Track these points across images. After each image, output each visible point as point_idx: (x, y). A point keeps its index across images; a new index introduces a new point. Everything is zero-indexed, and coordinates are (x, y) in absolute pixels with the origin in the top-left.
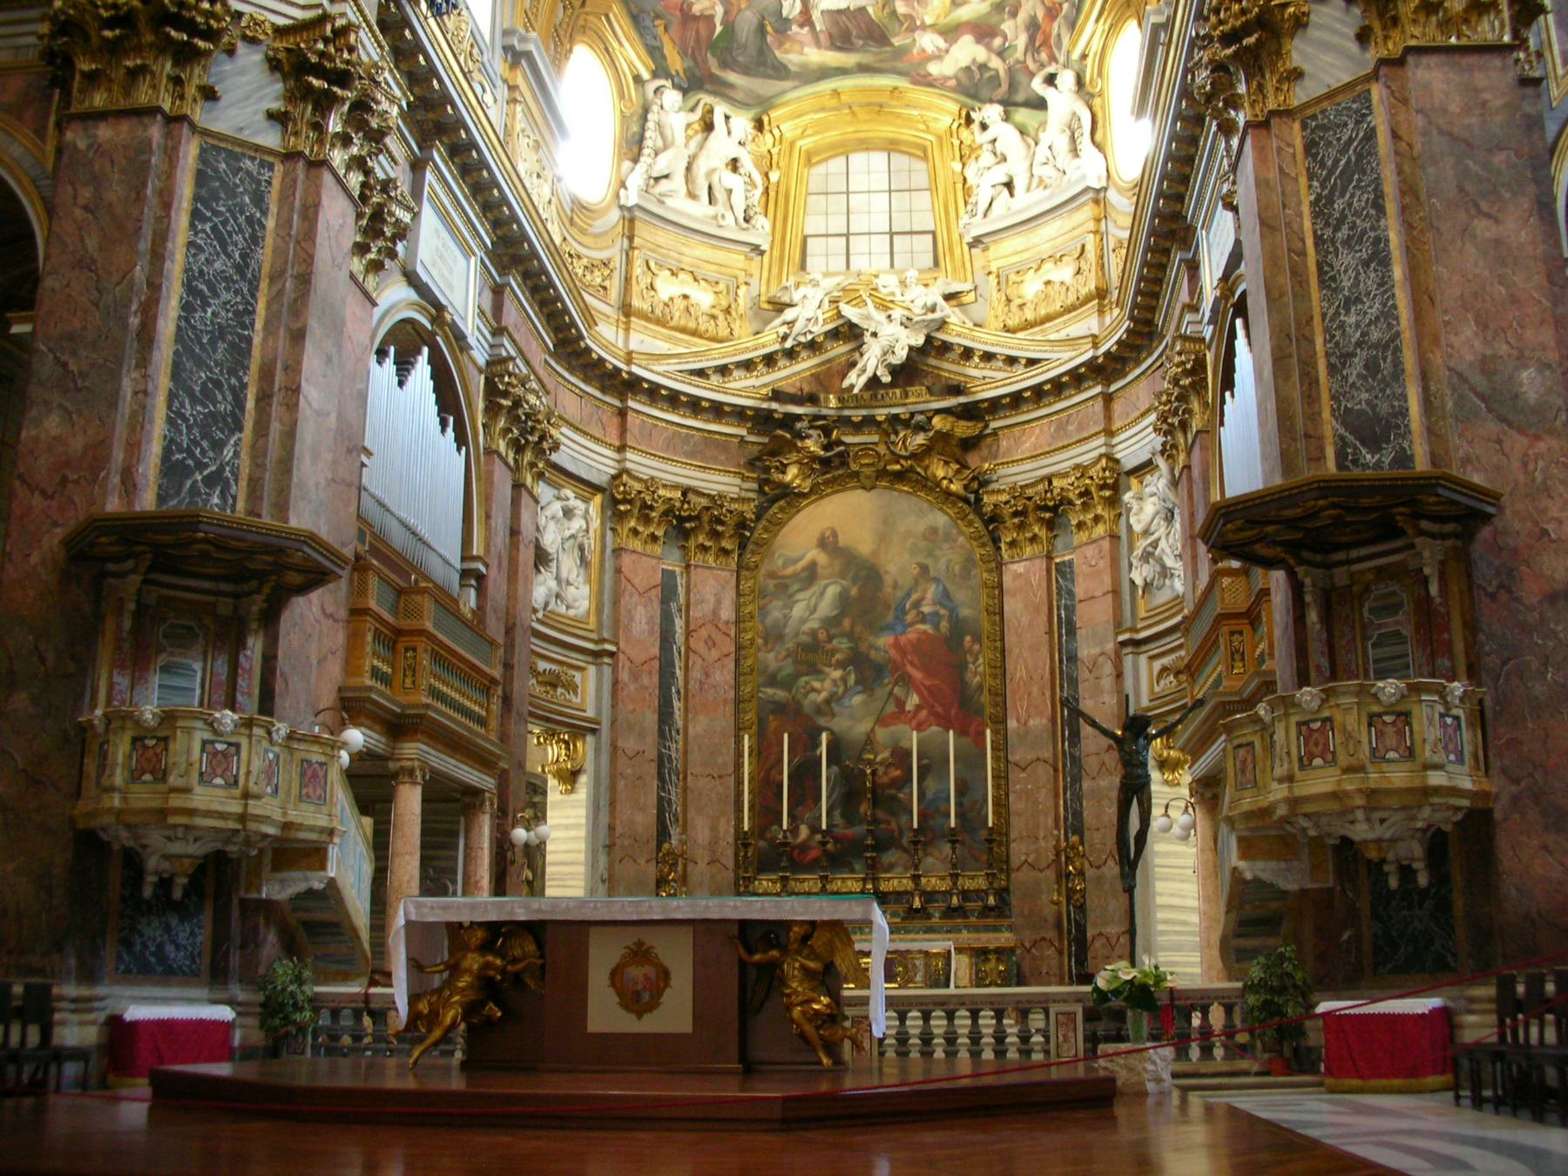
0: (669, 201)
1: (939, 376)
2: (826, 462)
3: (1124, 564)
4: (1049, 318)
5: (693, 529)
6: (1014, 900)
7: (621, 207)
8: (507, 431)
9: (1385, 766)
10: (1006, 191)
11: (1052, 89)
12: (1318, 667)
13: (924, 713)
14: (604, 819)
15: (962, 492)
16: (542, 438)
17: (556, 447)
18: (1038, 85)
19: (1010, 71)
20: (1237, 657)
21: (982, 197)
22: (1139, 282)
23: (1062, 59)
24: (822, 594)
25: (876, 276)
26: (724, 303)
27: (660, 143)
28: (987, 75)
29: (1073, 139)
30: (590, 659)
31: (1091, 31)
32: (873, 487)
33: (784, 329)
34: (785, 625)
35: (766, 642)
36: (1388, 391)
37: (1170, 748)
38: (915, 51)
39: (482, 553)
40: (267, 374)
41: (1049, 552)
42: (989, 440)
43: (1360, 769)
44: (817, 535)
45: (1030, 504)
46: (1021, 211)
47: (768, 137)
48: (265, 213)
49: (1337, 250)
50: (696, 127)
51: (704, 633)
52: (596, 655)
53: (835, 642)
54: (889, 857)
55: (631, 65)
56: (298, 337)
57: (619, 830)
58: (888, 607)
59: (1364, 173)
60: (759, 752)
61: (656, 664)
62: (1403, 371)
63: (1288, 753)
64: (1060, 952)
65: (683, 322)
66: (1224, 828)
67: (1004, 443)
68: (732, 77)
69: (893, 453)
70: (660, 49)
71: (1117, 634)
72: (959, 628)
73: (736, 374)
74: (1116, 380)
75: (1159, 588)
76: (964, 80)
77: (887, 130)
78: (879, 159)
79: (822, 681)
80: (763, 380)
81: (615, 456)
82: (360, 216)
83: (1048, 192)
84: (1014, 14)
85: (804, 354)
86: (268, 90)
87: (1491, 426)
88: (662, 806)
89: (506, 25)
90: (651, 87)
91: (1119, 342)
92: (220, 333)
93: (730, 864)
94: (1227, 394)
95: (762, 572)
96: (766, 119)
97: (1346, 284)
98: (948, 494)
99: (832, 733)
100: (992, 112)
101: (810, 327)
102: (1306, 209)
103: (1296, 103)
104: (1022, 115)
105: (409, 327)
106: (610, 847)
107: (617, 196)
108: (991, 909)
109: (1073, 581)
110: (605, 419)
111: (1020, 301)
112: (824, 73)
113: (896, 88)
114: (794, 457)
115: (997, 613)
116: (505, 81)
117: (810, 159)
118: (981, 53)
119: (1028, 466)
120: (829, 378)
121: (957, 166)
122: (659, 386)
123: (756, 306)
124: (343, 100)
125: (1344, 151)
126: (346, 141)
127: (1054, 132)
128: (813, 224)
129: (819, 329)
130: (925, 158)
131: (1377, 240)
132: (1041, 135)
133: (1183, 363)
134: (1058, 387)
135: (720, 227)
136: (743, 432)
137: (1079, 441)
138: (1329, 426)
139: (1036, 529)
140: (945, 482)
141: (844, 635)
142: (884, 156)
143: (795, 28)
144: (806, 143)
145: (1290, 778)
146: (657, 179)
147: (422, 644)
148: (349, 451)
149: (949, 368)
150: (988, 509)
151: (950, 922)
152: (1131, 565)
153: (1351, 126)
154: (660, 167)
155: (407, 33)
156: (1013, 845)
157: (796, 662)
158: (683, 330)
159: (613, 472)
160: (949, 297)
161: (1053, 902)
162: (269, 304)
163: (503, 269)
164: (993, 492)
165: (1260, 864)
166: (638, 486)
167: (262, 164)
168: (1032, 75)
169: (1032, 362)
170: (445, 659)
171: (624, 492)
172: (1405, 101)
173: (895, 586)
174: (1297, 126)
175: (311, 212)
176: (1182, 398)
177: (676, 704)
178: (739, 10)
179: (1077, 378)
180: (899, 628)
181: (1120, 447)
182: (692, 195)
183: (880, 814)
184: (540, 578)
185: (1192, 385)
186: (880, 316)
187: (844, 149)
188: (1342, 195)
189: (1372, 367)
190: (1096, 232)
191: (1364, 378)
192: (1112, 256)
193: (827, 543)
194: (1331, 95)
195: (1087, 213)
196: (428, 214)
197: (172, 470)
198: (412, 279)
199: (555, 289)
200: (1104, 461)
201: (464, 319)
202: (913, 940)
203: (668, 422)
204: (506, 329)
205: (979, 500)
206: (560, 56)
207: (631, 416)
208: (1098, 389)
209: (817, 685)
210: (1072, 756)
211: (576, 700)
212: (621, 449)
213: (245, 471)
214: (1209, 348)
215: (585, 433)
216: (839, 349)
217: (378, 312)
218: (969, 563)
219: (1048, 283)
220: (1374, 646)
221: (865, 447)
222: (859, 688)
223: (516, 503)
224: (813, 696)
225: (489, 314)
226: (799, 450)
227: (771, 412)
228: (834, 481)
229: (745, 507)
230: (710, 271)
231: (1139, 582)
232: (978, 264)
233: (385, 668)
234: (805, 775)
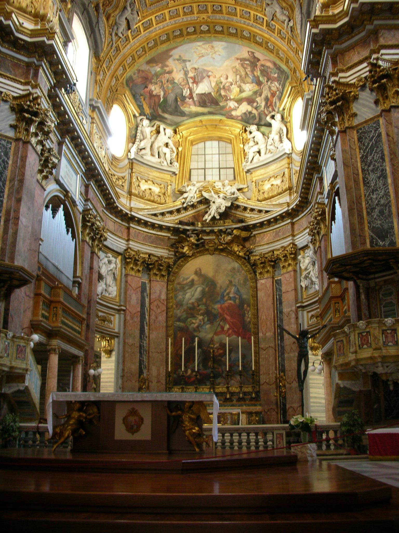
0: (145, 157)
1: (236, 216)
2: (197, 246)
3: (299, 280)
4: (273, 197)
5: (152, 268)
6: (262, 395)
7: (129, 159)
8: (89, 234)
9: (388, 348)
10: (258, 154)
11: (273, 120)
12: (365, 314)
13: (230, 331)
14: (121, 366)
15: (243, 255)
16: (101, 236)
17: (106, 239)
18: (268, 119)
19: (259, 114)
20: (337, 311)
21: (250, 156)
22: (303, 184)
23: (276, 110)
24: (196, 290)
25: (215, 183)
26: (163, 191)
27: (142, 137)
28: (251, 115)
29: (280, 137)
30: (117, 312)
31: (286, 101)
32: (213, 254)
33: (183, 200)
34: (183, 301)
35: (177, 307)
36: (387, 221)
37: (314, 343)
38: (227, 107)
39: (80, 275)
41: (273, 276)
42: (252, 238)
43: (380, 349)
44: (194, 270)
45: (267, 260)
46: (263, 161)
47: (178, 136)
48: (8, 159)
49: (369, 173)
50: (154, 132)
51: (155, 303)
52: (119, 311)
53: (200, 307)
54: (219, 380)
55: (132, 111)
56: (19, 201)
57: (126, 370)
58: (218, 295)
59: (378, 147)
60: (174, 344)
61: (139, 314)
62: (392, 214)
63: (355, 344)
64: (277, 413)
65: (149, 198)
66: (333, 370)
67: (258, 239)
68: (166, 116)
69: (220, 242)
70: (142, 106)
71: (296, 304)
72: (243, 302)
73: (167, 215)
74: (295, 218)
75: (311, 288)
76: (244, 117)
77: (218, 134)
78: (215, 143)
79: (196, 320)
80: (176, 217)
81: (126, 243)
82: (40, 160)
83: (272, 154)
84: (260, 95)
85: (190, 209)
86: (11, 117)
88: (141, 362)
89: (91, 97)
90: (139, 119)
91: (296, 205)
93: (164, 382)
94: (333, 222)
95: (176, 282)
96: (177, 130)
97: (373, 184)
98: (239, 256)
99: (199, 338)
100: (253, 128)
101: (192, 200)
102: (359, 160)
103: (355, 124)
104: (263, 129)
105: (56, 198)
106: (123, 377)
107: (127, 155)
108: (254, 398)
109: (281, 286)
110: (122, 230)
111: (262, 191)
112: (197, 115)
113: (221, 120)
114: (187, 243)
115: (256, 296)
116: (90, 116)
117: (192, 143)
118: (249, 108)
119: (266, 247)
120: (199, 217)
121: (242, 146)
122: (141, 219)
123: (174, 192)
124: (36, 121)
125: (371, 140)
126: (36, 135)
127: (274, 135)
128: (193, 165)
129: (195, 200)
130: (231, 143)
131: (383, 170)
132: (270, 135)
133: (318, 212)
134: (276, 220)
135: (162, 166)
136: (169, 235)
137: (283, 238)
138: (368, 232)
139: (269, 268)
140: (238, 252)
141: (203, 304)
142: (217, 142)
143: (187, 99)
144: (190, 138)
145: (356, 352)
146: (141, 150)
147: (59, 306)
148: (36, 240)
149: (239, 214)
150: (252, 261)
151: (240, 403)
152: (301, 280)
153: (373, 132)
154: (142, 145)
155: (57, 99)
156: (261, 376)
159: (125, 248)
160: (239, 190)
161: (275, 396)
162: (9, 190)
163: (88, 179)
164: (254, 256)
165: (346, 382)
166: (133, 253)
167: (8, 142)
168: (267, 116)
169: (267, 212)
170: (67, 311)
171: (129, 255)
172: (391, 124)
173: (221, 288)
174: (355, 132)
175: (24, 159)
176: (318, 224)
177: (146, 328)
178: (169, 93)
179: (282, 217)
180: (222, 302)
181: (297, 240)
182: (153, 155)
183: (216, 366)
184: (100, 284)
185: (321, 219)
186: (216, 196)
187: (204, 140)
188: (371, 155)
189: (381, 212)
190: (288, 168)
191: (379, 216)
192: (294, 176)
193: (198, 273)
194: (366, 122)
195: (285, 162)
196: (64, 160)
198: (58, 182)
199: (106, 186)
200: (291, 245)
201: (75, 196)
202: (226, 409)
203: (144, 231)
204: (89, 199)
205: (249, 258)
206: (109, 108)
207: (131, 229)
208: (289, 221)
209: (194, 321)
210: (281, 345)
211: (112, 326)
212: (128, 240)
214: (327, 207)
215: (115, 235)
216: (202, 207)
217: (46, 193)
218: (246, 280)
219: (272, 185)
220: (384, 307)
221: (211, 240)
222: (208, 322)
223: (92, 258)
224: (193, 325)
225: (84, 194)
226: (188, 241)
227: (179, 228)
228: (200, 251)
229: (170, 261)
230: (159, 181)
231: (304, 286)
232: (249, 179)
233: (46, 314)
234: (190, 352)
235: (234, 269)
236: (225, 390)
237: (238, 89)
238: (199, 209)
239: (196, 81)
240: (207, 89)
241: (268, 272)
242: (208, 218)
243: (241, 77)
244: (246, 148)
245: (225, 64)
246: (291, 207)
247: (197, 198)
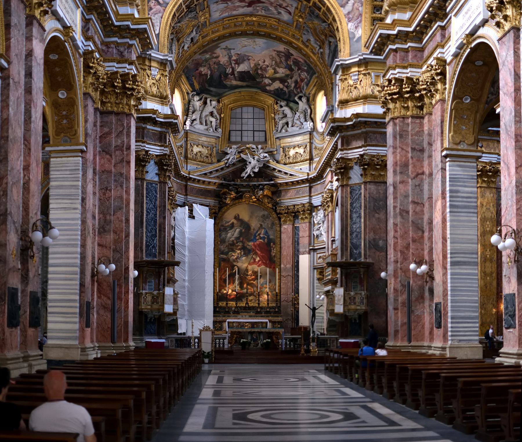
10: (286, 126)
26: (210, 153)
33: (226, 161)
35: (221, 243)
40: (160, 226)
64: (292, 322)
72: (270, 241)
77: (254, 103)
78: (251, 109)
87: (374, 250)
91: (314, 176)
92: (152, 219)
95: (220, 225)
99: (238, 267)
100: (283, 103)
102: (349, 204)
108: (277, 312)
112: (237, 87)
118: (281, 86)
119: (289, 201)
121: (273, 115)
122: (195, 179)
123: (217, 153)
125: (356, 195)
134: (298, 182)
138: (349, 244)
141: (241, 242)
150: (278, 211)
157: (228, 248)
158: (200, 162)
169: (291, 175)
173: (254, 229)
174: (349, 188)
179: (303, 182)
185: (330, 200)
187: (242, 107)
189: (357, 236)
193: (237, 218)
197: (147, 246)
205: (276, 208)
208: (308, 185)
209: (234, 254)
212: (186, 195)
213: (158, 245)
216: (241, 165)
218: (273, 224)
224: (232, 257)
231: (315, 235)
232: (278, 144)
235: (264, 215)
236: (257, 305)
237: (273, 71)
238: (238, 166)
239: (238, 62)
240: (246, 68)
241: (290, 220)
242: (244, 175)
243: (276, 62)
244: (277, 117)
245: (263, 53)
246: (310, 177)
247: (237, 158)
